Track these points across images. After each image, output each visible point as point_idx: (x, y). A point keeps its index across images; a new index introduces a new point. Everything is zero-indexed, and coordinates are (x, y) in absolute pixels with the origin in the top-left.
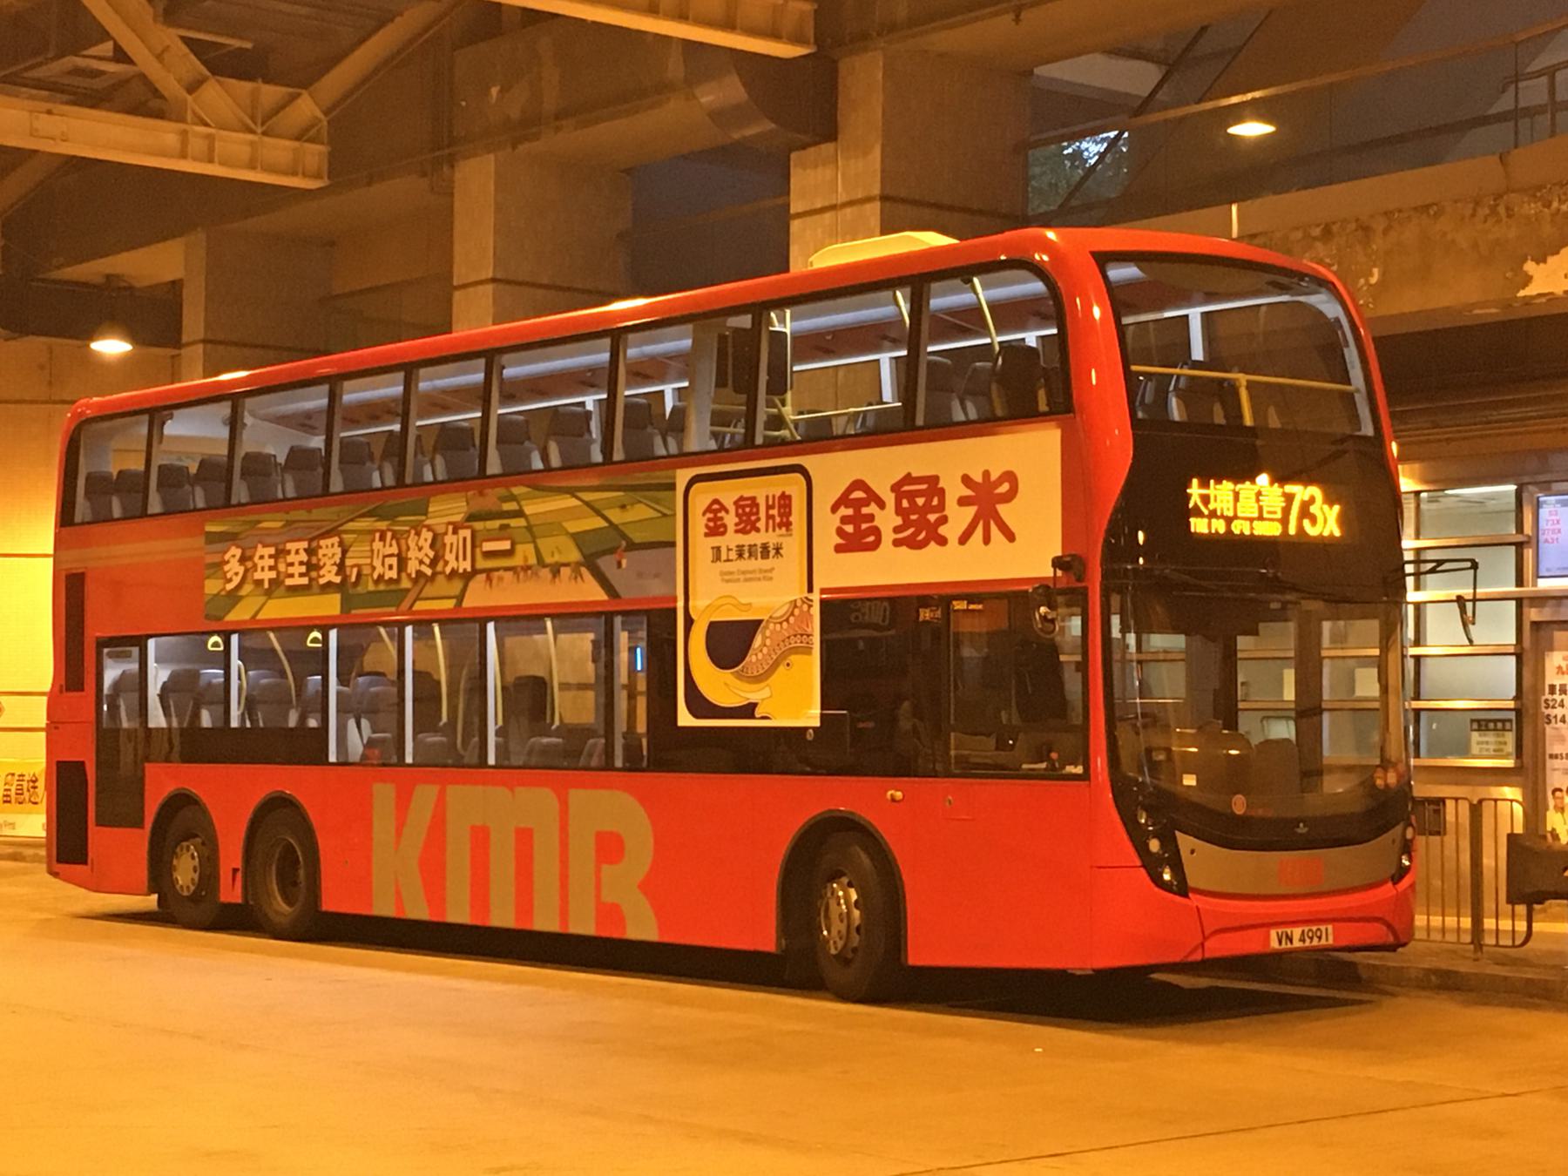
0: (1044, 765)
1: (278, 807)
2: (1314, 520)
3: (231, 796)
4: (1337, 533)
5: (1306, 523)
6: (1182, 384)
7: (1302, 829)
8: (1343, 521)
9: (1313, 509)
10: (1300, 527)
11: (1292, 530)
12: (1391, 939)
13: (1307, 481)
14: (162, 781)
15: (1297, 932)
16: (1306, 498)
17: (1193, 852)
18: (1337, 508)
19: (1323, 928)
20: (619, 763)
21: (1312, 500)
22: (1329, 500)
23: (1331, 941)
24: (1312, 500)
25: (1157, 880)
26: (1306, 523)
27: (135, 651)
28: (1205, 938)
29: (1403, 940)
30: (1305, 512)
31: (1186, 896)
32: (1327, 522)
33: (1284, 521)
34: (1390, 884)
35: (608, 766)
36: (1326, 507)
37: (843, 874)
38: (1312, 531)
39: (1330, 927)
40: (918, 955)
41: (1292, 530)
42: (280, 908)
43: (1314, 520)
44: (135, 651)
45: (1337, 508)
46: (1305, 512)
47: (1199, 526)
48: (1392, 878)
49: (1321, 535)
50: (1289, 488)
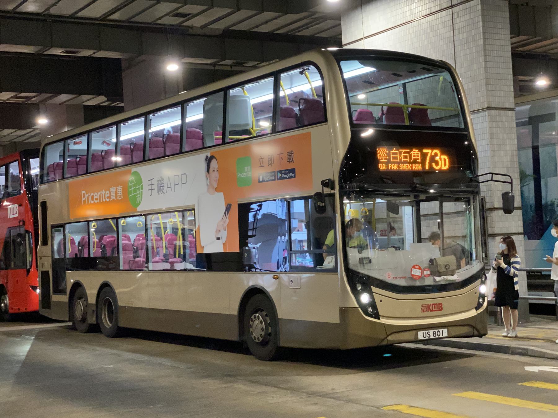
1: (105, 286)
2: (437, 163)
5: (434, 164)
9: (437, 158)
10: (431, 166)
11: (427, 167)
12: (476, 333)
13: (432, 146)
15: (431, 332)
16: (433, 154)
17: (381, 301)
19: (441, 330)
21: (436, 155)
24: (436, 155)
26: (434, 164)
27: (62, 229)
28: (388, 336)
29: (482, 332)
31: (379, 319)
33: (423, 163)
34: (474, 310)
37: (262, 311)
41: (427, 167)
42: (107, 323)
46: (433, 159)
47: (382, 167)
50: (425, 151)
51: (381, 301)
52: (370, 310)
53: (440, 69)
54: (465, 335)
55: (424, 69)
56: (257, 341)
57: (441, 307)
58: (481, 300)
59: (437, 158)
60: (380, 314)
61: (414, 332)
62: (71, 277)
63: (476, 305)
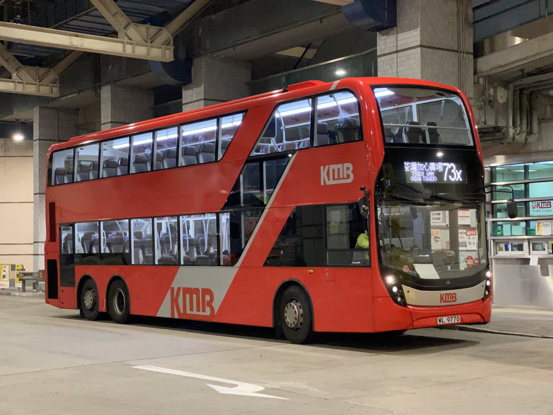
0: (359, 263)
2: (453, 176)
3: (101, 276)
4: (461, 180)
5: (450, 176)
6: (407, 130)
7: (448, 283)
8: (462, 176)
9: (453, 171)
10: (448, 178)
11: (445, 179)
12: (482, 321)
14: (80, 271)
17: (408, 292)
18: (461, 171)
20: (222, 263)
21: (452, 168)
22: (458, 169)
23: (460, 321)
24: (452, 168)
25: (396, 301)
26: (450, 176)
27: (71, 228)
30: (450, 173)
32: (457, 176)
35: (219, 265)
36: (457, 171)
38: (452, 179)
39: (459, 316)
40: (318, 328)
41: (445, 179)
43: (453, 176)
44: (71, 228)
45: (461, 171)
46: (450, 173)
48: (483, 299)
49: (455, 181)
51: (408, 292)
52: (399, 299)
53: (452, 95)
54: (472, 322)
55: (438, 94)
56: (289, 325)
57: (455, 297)
58: (487, 293)
59: (453, 171)
60: (408, 302)
61: (435, 318)
62: (80, 271)
63: (482, 297)
